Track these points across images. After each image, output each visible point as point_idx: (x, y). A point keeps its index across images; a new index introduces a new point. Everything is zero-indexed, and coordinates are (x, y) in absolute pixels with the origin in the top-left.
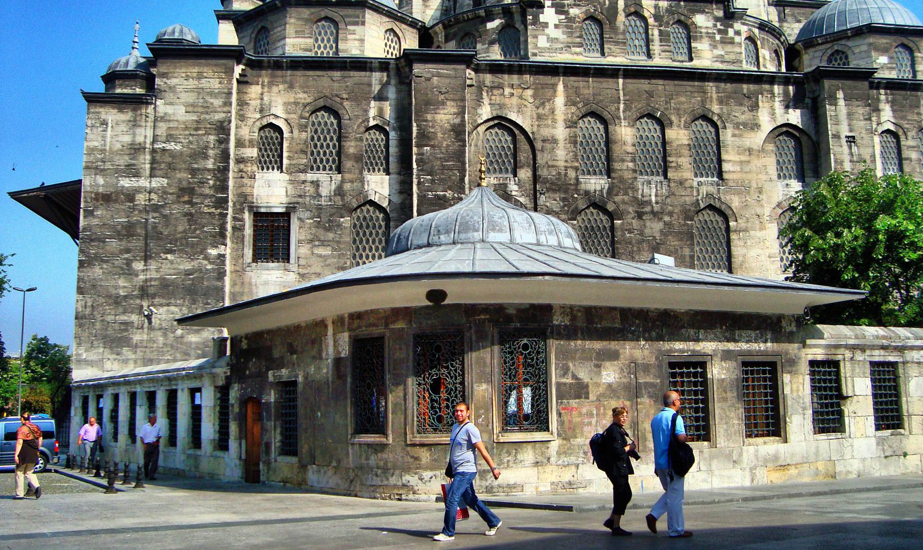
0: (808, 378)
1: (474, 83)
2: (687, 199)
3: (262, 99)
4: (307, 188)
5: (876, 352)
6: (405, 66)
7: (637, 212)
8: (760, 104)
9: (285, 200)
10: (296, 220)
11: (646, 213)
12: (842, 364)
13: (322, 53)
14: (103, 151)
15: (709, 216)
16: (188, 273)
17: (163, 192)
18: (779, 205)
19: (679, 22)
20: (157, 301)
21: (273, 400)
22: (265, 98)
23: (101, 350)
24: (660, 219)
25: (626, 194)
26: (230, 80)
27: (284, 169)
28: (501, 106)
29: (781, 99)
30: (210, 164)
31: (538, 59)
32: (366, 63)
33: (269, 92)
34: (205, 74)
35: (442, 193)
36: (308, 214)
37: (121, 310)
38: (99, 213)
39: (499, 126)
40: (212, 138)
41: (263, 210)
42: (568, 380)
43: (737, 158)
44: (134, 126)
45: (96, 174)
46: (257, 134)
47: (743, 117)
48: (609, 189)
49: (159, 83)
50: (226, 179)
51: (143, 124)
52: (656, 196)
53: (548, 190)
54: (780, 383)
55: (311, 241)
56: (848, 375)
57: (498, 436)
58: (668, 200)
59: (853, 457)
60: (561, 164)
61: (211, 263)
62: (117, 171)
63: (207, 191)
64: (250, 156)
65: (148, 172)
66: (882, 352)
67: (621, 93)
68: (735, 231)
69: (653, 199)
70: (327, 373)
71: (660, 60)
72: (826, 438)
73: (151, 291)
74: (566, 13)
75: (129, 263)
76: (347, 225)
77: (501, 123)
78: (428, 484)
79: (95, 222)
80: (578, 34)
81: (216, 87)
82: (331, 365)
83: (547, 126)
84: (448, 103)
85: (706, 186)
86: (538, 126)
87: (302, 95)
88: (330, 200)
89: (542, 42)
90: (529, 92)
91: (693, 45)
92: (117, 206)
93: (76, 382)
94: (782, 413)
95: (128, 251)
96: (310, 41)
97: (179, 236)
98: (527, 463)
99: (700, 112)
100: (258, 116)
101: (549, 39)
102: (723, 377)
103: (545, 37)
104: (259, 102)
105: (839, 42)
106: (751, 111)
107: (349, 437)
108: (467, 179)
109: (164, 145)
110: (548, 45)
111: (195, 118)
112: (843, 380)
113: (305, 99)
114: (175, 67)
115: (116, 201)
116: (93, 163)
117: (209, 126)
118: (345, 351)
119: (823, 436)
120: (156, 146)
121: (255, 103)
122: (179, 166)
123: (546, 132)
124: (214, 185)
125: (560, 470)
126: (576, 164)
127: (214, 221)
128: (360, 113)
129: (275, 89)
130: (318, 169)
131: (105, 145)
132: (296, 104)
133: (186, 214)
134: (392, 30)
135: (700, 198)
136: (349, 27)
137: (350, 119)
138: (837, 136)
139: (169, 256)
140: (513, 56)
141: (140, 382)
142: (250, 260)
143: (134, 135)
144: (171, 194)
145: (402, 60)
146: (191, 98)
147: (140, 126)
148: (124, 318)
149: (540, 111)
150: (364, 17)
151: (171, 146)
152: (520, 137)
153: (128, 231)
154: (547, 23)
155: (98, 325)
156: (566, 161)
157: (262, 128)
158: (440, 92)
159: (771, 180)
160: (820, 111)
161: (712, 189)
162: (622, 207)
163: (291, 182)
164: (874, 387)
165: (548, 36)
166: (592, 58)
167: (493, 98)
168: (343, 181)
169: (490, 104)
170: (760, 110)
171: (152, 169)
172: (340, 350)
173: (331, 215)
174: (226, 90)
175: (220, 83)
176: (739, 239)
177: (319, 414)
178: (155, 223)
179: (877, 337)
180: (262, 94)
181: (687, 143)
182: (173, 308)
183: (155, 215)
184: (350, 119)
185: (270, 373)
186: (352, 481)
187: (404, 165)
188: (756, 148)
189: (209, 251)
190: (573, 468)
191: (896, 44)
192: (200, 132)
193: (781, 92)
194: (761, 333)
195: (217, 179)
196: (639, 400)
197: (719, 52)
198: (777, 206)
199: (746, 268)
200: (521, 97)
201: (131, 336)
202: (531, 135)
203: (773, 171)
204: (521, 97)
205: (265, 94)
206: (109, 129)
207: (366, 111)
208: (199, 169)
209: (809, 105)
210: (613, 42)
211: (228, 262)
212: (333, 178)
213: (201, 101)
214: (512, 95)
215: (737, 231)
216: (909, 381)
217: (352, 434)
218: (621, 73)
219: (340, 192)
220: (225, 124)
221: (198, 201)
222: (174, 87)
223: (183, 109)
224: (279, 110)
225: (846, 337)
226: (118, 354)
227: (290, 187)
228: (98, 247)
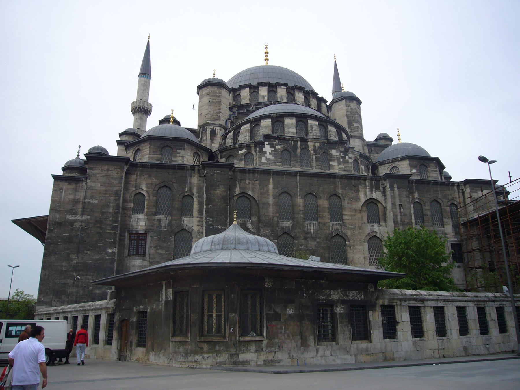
0: (380, 313)
1: (233, 178)
2: (327, 231)
3: (136, 181)
4: (155, 223)
5: (411, 302)
6: (202, 169)
7: (304, 237)
8: (360, 190)
9: (144, 228)
10: (149, 237)
11: (309, 237)
12: (396, 307)
13: (165, 161)
15: (337, 239)
16: (97, 260)
17: (87, 222)
18: (369, 234)
20: (81, 273)
21: (135, 321)
22: (138, 181)
24: (315, 240)
25: (300, 228)
26: (122, 172)
27: (145, 213)
29: (369, 187)
30: (111, 210)
32: (185, 167)
33: (139, 178)
34: (111, 169)
35: (217, 226)
38: (56, 231)
40: (112, 198)
42: (271, 312)
43: (350, 213)
44: (75, 191)
45: (55, 213)
46: (133, 197)
47: (352, 195)
48: (292, 226)
49: (89, 172)
50: (117, 218)
51: (80, 190)
52: (313, 230)
54: (368, 315)
55: (156, 247)
56: (399, 312)
57: (239, 338)
58: (319, 232)
59: (402, 351)
60: (272, 215)
61: (108, 256)
63: (109, 222)
64: (129, 207)
65: (80, 213)
66: (414, 302)
67: (298, 183)
68: (349, 246)
69: (312, 231)
70: (162, 308)
71: (315, 169)
72: (389, 341)
74: (275, 148)
75: (68, 255)
76: (173, 240)
77: (244, 195)
78: (206, 360)
79: (54, 235)
80: (280, 157)
81: (115, 175)
82: (163, 304)
84: (221, 186)
85: (335, 226)
86: (261, 197)
88: (165, 228)
89: (264, 160)
90: (257, 182)
93: (37, 312)
94: (369, 329)
95: (68, 249)
98: (252, 351)
99: (334, 193)
100: (134, 189)
102: (342, 312)
103: (265, 158)
104: (135, 182)
105: (395, 163)
107: (171, 338)
108: (228, 220)
109: (89, 200)
110: (266, 162)
111: (105, 189)
112: (396, 314)
113: (156, 182)
116: (54, 207)
117: (111, 193)
118: (170, 297)
119: (388, 340)
120: (86, 201)
121: (133, 183)
124: (112, 220)
125: (267, 354)
126: (278, 215)
129: (143, 177)
131: (61, 199)
132: (152, 184)
134: (197, 152)
135: (333, 231)
136: (177, 151)
137: (176, 192)
139: (88, 252)
140: (250, 166)
141: (71, 312)
142: (127, 255)
143: (75, 195)
144: (91, 223)
147: (79, 191)
149: (262, 190)
150: (184, 146)
151: (93, 201)
153: (69, 240)
154: (266, 152)
156: (273, 213)
157: (136, 195)
158: (217, 181)
159: (365, 223)
161: (338, 227)
162: (298, 235)
163: (148, 219)
164: (411, 318)
165: (266, 157)
167: (241, 184)
168: (172, 220)
169: (239, 187)
170: (360, 192)
172: (168, 297)
174: (120, 177)
175: (117, 173)
176: (351, 250)
177: (157, 327)
178: (82, 236)
179: (411, 295)
180: (136, 179)
181: (327, 206)
182: (89, 277)
184: (176, 192)
185: (135, 308)
186: (171, 359)
187: (200, 213)
189: (108, 250)
190: (273, 353)
191: (419, 164)
192: (107, 195)
193: (369, 184)
194: (358, 292)
196: (303, 322)
197: (342, 166)
198: (368, 235)
199: (354, 263)
200: (253, 184)
201: (67, 290)
202: (257, 201)
203: (365, 219)
204: (253, 184)
205: (138, 179)
206: (64, 192)
209: (382, 190)
210: (295, 161)
211: (116, 255)
212: (167, 218)
213: (108, 181)
214: (249, 183)
215: (350, 246)
216: (427, 315)
217: (171, 337)
218: (298, 175)
219: (170, 224)
220: (119, 192)
221: (103, 227)
222: (96, 174)
224: (144, 187)
225: (397, 294)
226: (60, 298)
227: (147, 222)
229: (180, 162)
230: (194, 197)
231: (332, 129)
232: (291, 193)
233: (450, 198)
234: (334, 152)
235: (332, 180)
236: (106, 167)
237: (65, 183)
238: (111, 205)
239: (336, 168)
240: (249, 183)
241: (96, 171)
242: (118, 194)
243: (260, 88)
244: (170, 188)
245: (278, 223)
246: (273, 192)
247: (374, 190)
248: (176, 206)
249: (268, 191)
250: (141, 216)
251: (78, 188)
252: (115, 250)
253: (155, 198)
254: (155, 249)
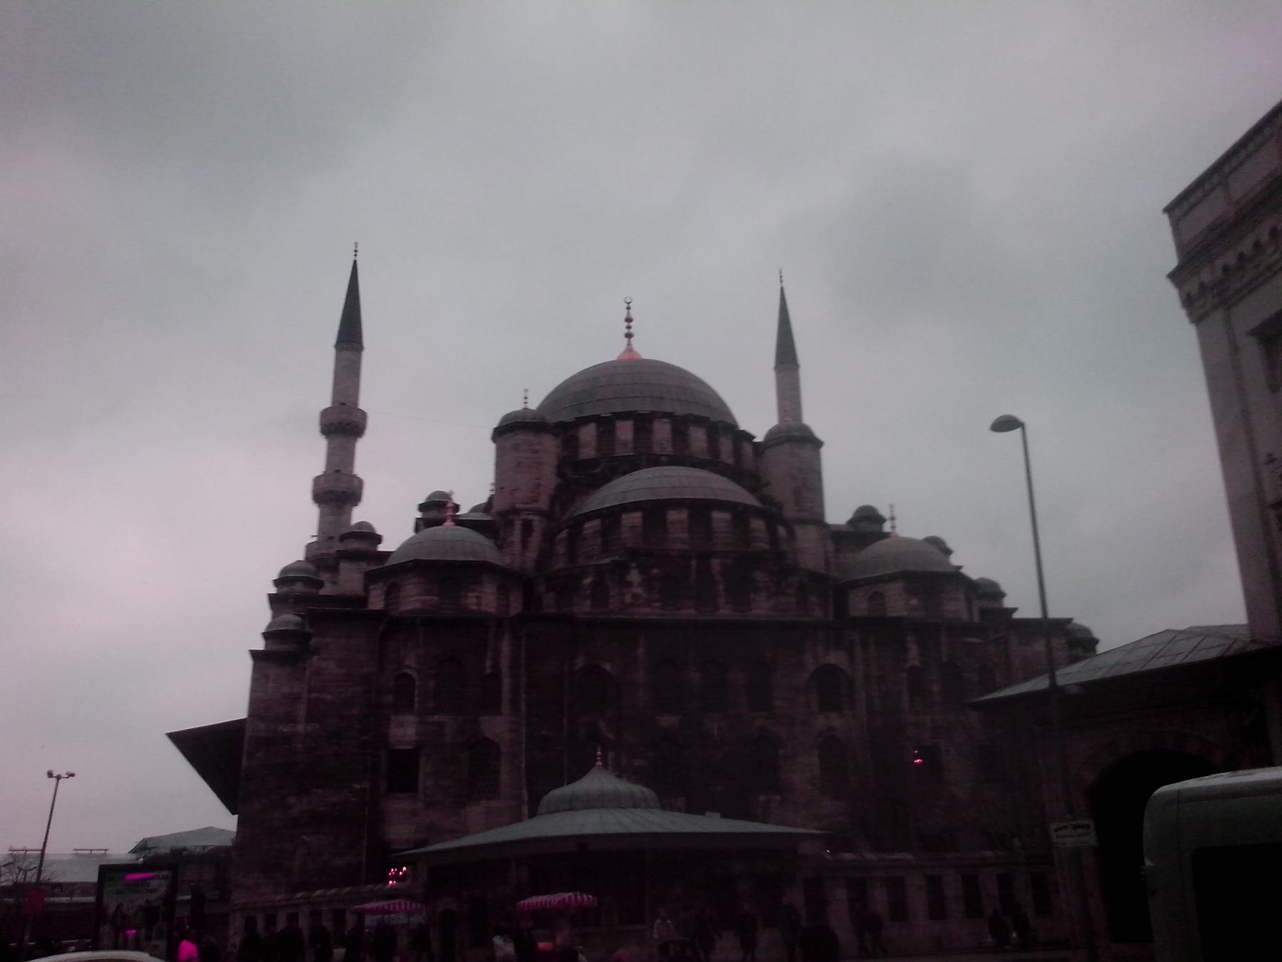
69: (716, 732)
71: (725, 612)
89: (628, 599)
101: (635, 597)
229: (474, 608)
231: (758, 524)
234: (759, 576)
243: (619, 424)
250: (411, 719)
252: (366, 785)
253: (431, 684)
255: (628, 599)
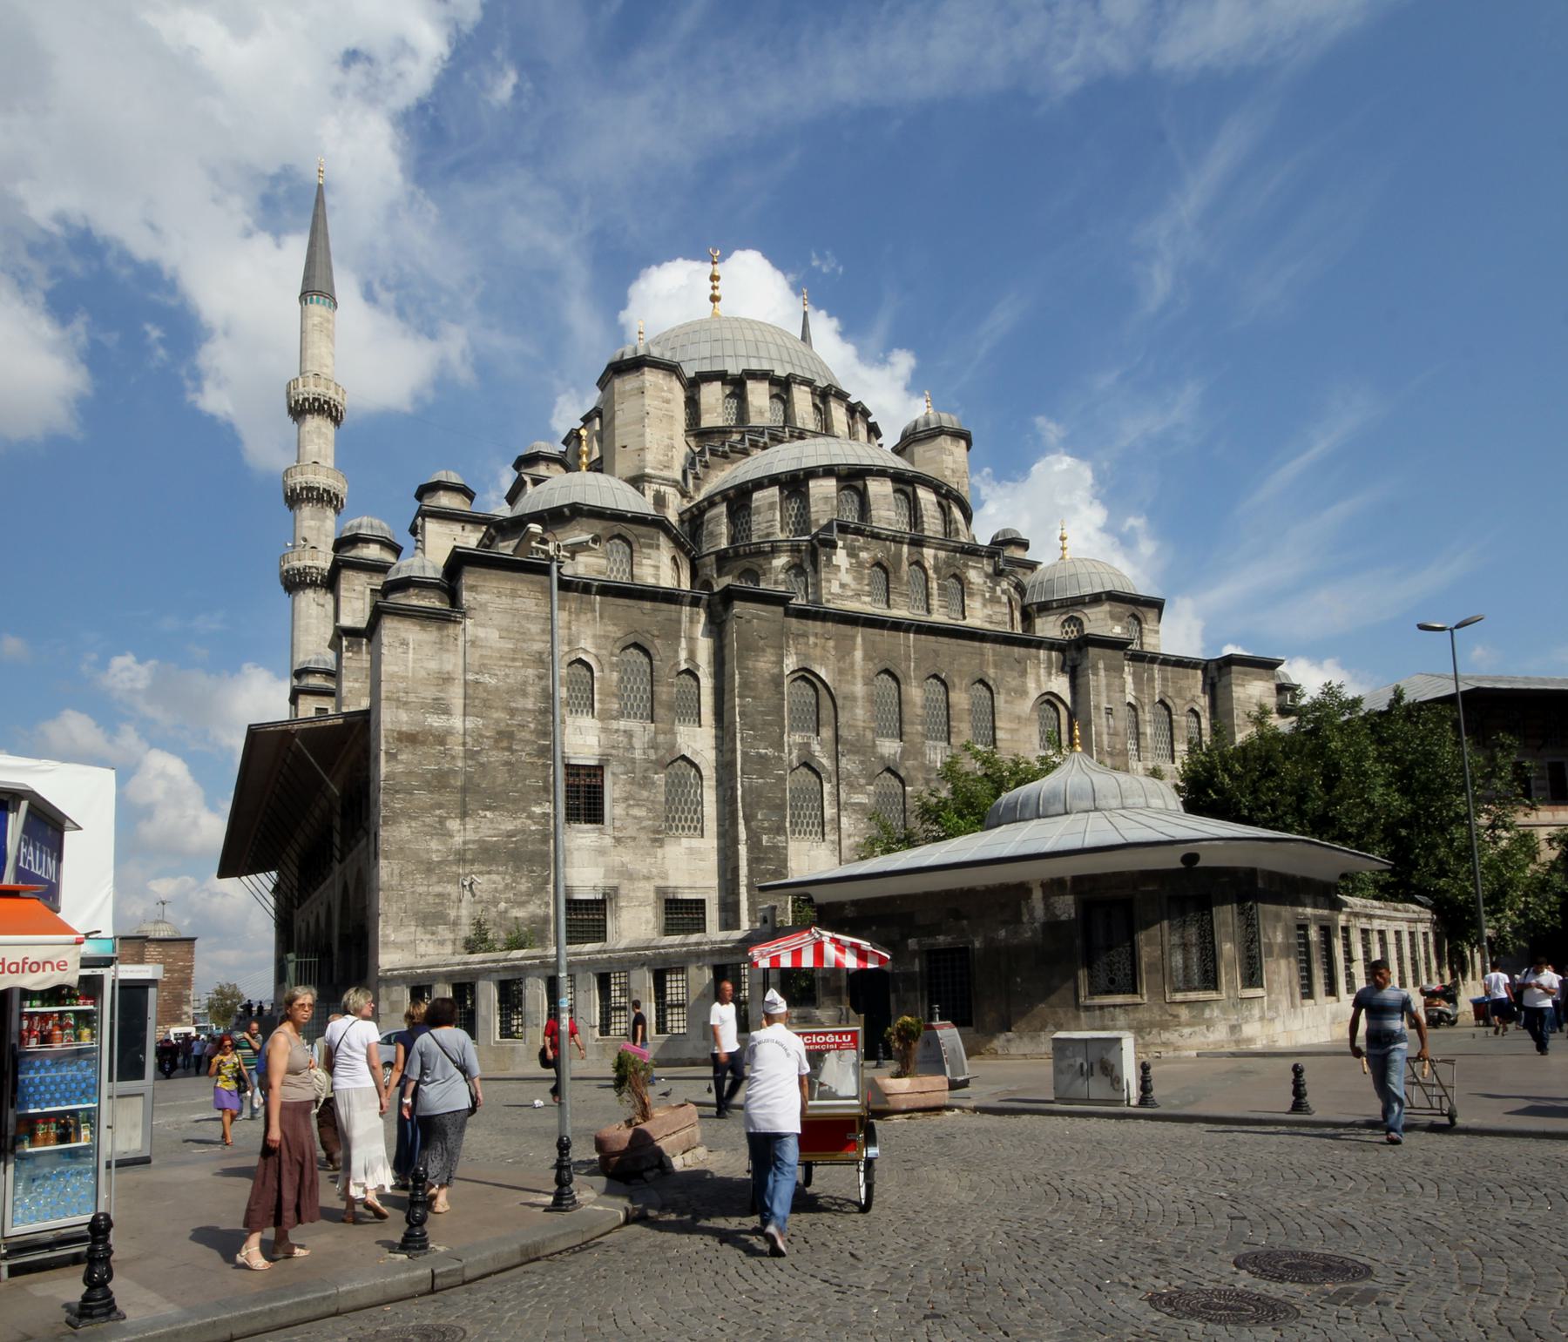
3: (570, 628)
9: (597, 750)
14: (404, 678)
16: (510, 835)
19: (955, 576)
20: (476, 867)
23: (413, 929)
28: (807, 657)
31: (831, 605)
36: (621, 769)
37: (434, 879)
39: (803, 678)
40: (531, 672)
41: (573, 762)
45: (397, 708)
50: (546, 725)
53: (849, 752)
61: (535, 823)
62: (423, 706)
71: (939, 617)
73: (469, 856)
74: (855, 556)
75: (442, 820)
77: (806, 675)
80: (866, 582)
83: (848, 682)
84: (769, 651)
87: (610, 628)
90: (831, 643)
91: (966, 602)
92: (425, 749)
95: (440, 806)
96: (604, 562)
97: (498, 789)
100: (566, 649)
101: (843, 586)
106: (1021, 676)
111: (511, 646)
114: (485, 580)
115: (423, 743)
122: (495, 705)
123: (845, 688)
127: (537, 773)
128: (671, 654)
129: (583, 618)
130: (629, 717)
132: (606, 637)
133: (507, 763)
136: (644, 550)
138: (1097, 707)
139: (488, 814)
145: (717, 597)
146: (505, 621)
147: (448, 650)
148: (438, 889)
149: (841, 664)
151: (486, 679)
152: (823, 692)
153: (439, 781)
155: (408, 899)
157: (570, 664)
160: (1080, 681)
162: (913, 773)
163: (605, 730)
166: (879, 610)
171: (465, 706)
173: (646, 770)
180: (570, 622)
182: (495, 877)
183: (470, 762)
188: (1023, 715)
192: (517, 664)
195: (539, 722)
197: (988, 611)
200: (824, 648)
204: (824, 648)
206: (411, 651)
207: (677, 652)
208: (517, 709)
219: (654, 745)
223: (495, 634)
226: (433, 934)
228: (404, 800)
230: (700, 674)
232: (900, 675)
233: (1189, 696)
235: (977, 644)
236: (509, 585)
237: (412, 627)
238: (530, 689)
239: (978, 616)
240: (816, 645)
241: (483, 598)
242: (542, 661)
244: (646, 652)
245: (874, 745)
246: (864, 670)
247: (1054, 671)
248: (664, 697)
249: (852, 664)
251: (445, 640)
253: (615, 676)
254: (624, 805)
255: (835, 588)
